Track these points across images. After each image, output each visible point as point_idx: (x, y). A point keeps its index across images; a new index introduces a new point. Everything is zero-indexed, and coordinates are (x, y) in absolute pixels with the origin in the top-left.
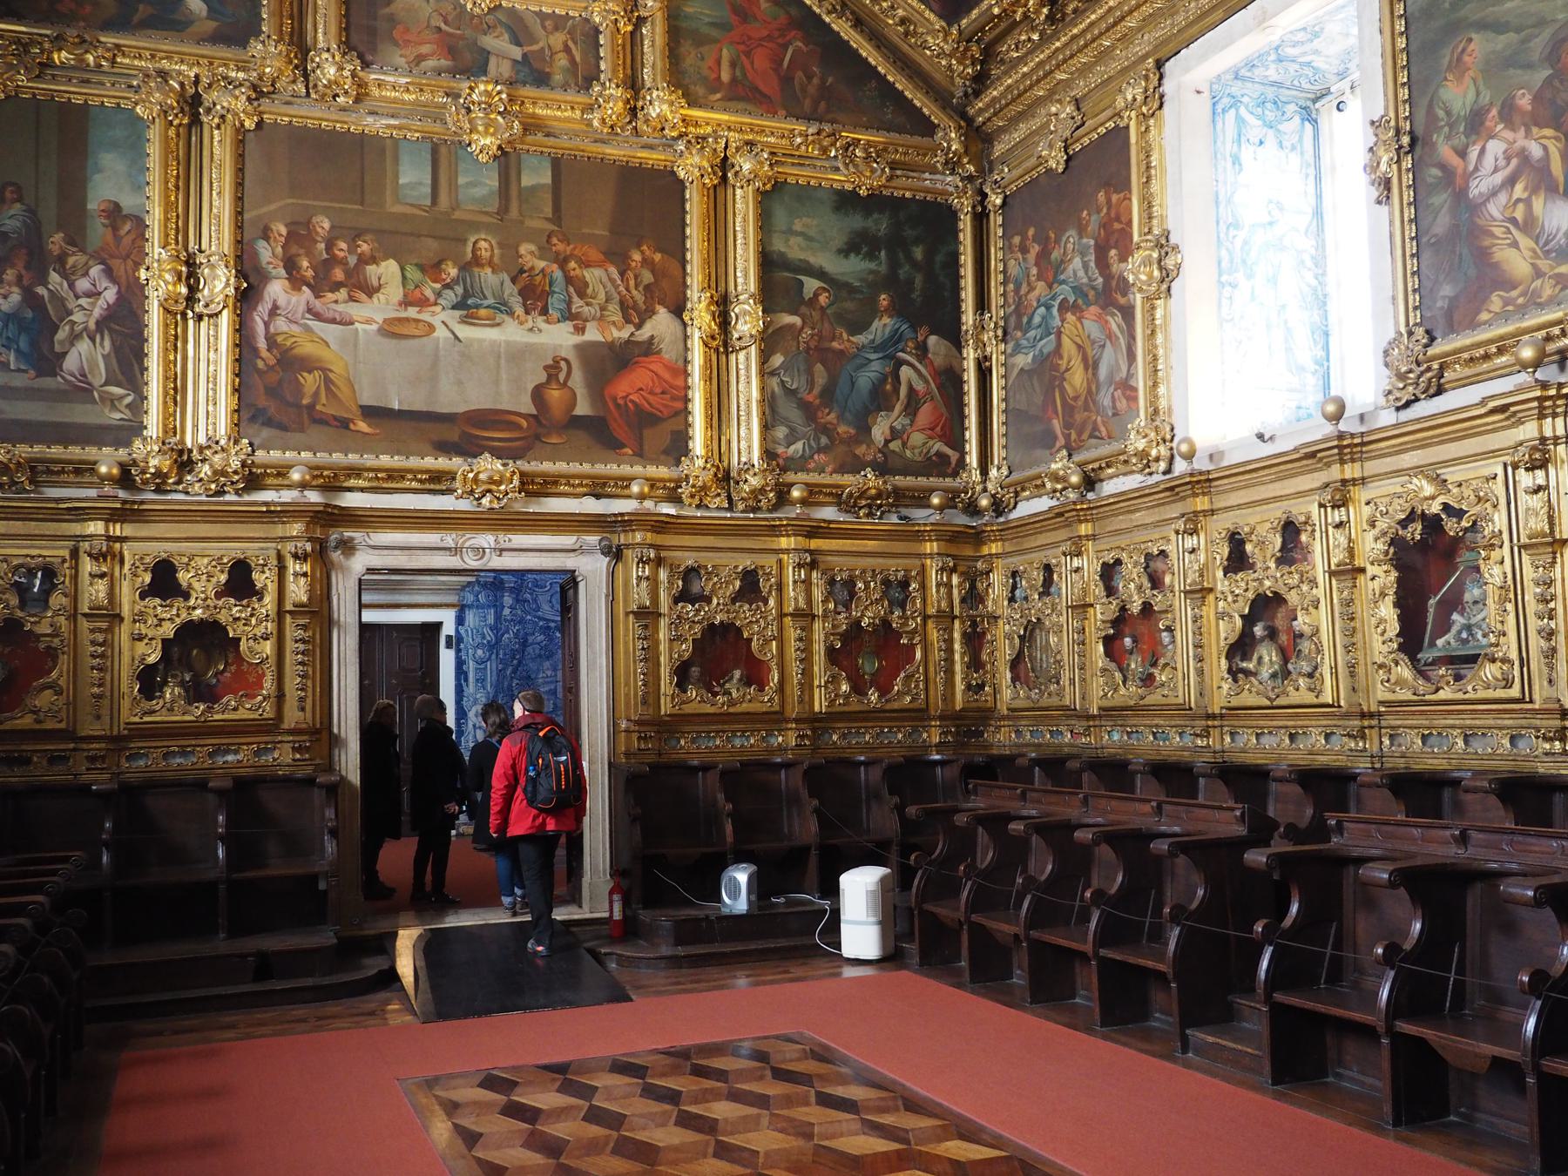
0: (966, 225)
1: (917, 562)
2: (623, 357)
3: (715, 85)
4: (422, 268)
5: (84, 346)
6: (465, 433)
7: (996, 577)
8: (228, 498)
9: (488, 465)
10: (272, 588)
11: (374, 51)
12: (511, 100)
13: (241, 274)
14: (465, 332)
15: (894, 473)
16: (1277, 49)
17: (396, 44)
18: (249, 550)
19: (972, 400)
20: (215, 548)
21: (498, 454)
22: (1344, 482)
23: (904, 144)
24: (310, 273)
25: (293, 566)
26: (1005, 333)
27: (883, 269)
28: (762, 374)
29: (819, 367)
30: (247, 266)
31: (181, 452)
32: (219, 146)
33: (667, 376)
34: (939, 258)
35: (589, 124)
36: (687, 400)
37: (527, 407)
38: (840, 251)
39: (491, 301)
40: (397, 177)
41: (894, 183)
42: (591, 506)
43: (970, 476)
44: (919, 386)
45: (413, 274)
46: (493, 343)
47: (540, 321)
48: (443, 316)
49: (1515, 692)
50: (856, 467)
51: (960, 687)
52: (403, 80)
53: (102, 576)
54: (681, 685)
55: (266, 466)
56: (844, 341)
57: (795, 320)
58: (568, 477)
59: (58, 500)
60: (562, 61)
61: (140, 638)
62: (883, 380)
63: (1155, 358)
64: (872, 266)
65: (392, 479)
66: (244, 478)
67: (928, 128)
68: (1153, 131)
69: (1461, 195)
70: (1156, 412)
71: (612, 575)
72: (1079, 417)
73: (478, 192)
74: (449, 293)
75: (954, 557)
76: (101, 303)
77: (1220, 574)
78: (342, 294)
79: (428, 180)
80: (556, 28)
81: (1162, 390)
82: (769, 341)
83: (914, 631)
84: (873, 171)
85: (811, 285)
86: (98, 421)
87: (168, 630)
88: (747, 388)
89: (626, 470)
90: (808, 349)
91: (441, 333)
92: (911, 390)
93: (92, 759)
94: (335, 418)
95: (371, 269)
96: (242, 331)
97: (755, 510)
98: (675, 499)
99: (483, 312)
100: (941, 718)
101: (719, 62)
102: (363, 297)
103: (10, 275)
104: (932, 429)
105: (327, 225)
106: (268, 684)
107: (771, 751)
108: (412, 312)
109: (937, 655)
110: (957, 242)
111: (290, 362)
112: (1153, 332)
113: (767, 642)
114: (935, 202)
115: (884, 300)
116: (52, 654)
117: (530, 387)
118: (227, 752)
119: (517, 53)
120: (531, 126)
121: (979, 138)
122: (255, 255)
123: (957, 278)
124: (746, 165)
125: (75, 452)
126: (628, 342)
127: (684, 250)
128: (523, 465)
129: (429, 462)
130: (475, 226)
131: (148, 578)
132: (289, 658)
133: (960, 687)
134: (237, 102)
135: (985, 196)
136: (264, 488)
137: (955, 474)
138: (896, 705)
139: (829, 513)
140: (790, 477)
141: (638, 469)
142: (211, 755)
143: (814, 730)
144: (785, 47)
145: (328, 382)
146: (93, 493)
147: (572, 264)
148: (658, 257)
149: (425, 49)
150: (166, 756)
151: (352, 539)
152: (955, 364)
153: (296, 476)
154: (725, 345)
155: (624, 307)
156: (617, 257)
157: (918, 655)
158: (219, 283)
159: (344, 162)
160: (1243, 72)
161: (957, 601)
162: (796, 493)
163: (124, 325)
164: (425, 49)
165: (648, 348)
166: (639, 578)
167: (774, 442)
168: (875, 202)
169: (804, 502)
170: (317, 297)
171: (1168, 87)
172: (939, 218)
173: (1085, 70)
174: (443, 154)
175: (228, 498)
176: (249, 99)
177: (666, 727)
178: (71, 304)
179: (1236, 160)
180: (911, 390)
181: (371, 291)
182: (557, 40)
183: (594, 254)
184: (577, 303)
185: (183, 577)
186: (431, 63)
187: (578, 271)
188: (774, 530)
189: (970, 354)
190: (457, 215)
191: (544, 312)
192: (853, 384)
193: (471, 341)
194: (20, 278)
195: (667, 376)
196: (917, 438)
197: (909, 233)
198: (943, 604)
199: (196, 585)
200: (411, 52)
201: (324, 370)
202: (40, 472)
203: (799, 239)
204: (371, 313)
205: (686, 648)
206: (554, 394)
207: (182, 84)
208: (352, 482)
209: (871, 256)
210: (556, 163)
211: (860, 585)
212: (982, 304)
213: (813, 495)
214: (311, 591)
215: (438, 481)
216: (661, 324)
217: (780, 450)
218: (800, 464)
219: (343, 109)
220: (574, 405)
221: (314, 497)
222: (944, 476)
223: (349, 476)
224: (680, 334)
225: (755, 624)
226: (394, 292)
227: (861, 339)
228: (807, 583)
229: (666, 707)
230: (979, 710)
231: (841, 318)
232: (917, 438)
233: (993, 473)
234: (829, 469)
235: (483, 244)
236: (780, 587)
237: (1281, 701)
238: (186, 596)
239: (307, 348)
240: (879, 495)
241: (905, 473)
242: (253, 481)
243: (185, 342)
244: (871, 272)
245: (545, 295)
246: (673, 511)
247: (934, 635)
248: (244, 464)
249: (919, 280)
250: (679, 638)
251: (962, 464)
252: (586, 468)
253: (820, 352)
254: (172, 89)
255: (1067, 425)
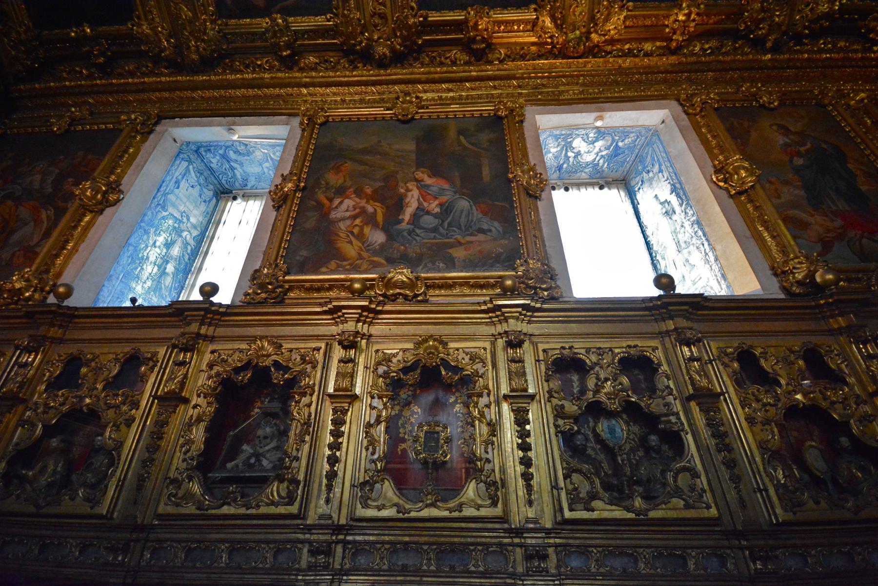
16: (227, 147)
22: (198, 335)
49: (294, 509)
171: (158, 128)
179: (177, 183)
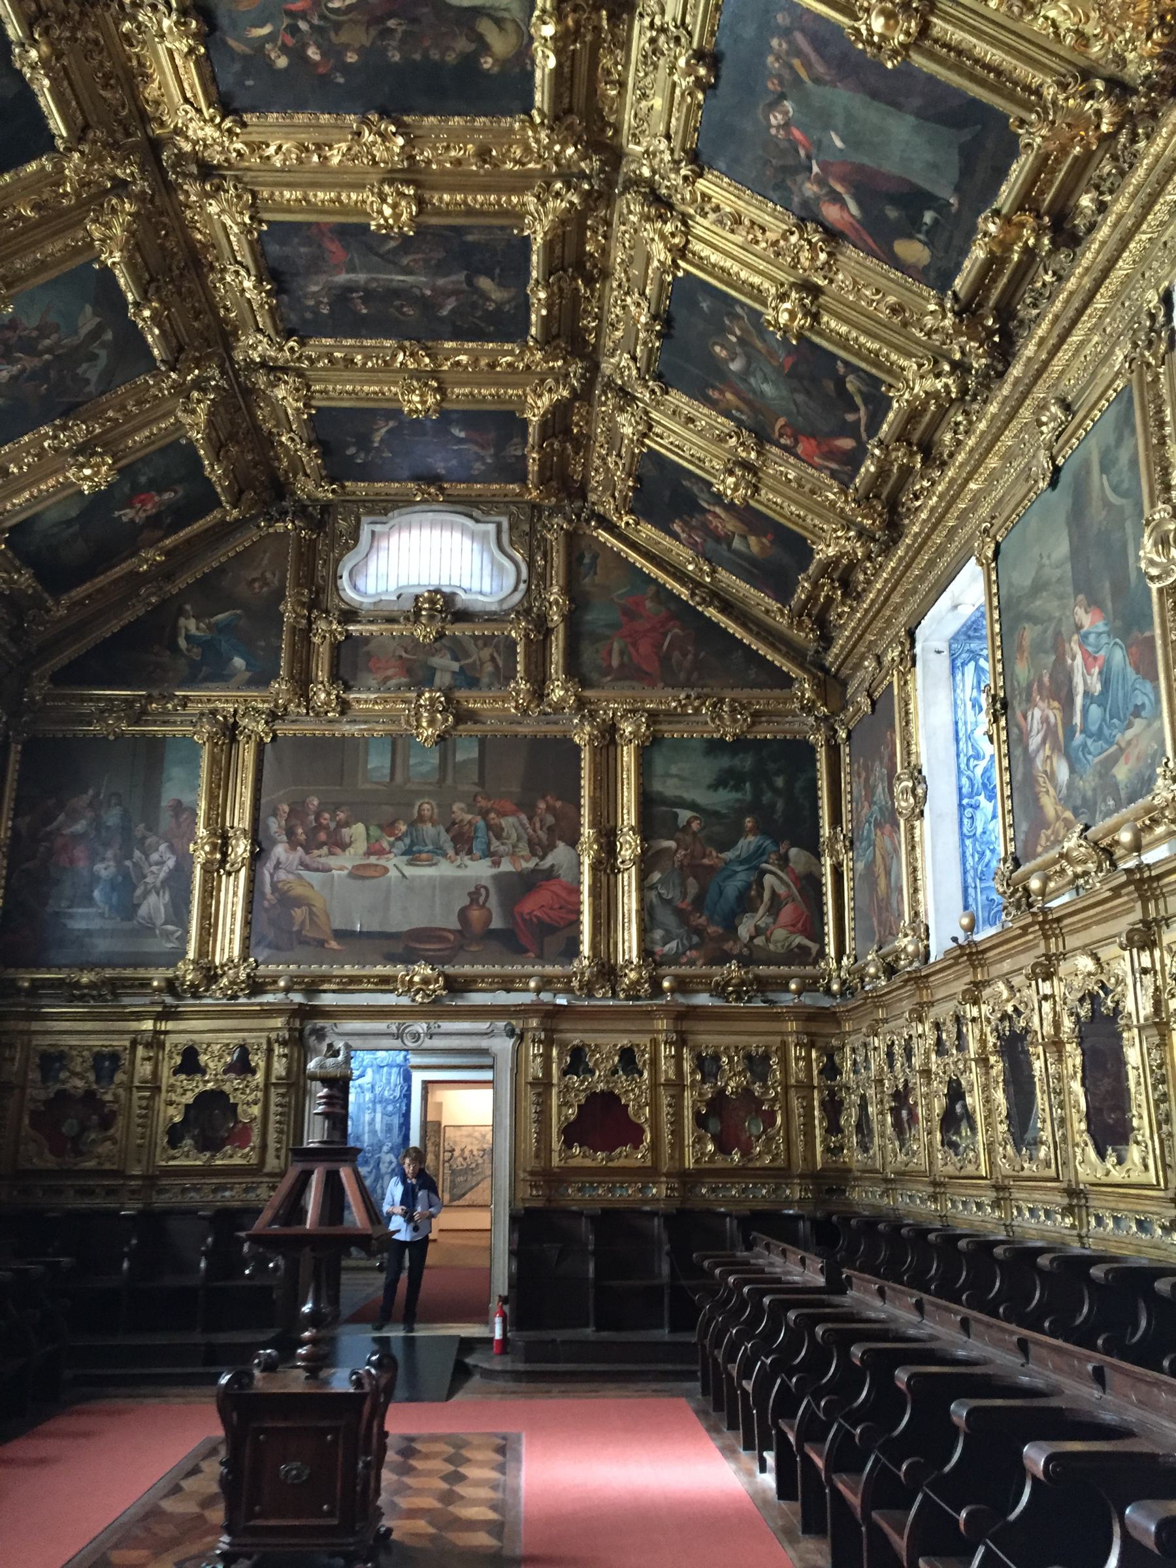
0: (822, 754)
1: (779, 1039)
2: (529, 882)
3: (608, 670)
4: (380, 827)
5: (152, 898)
6: (406, 946)
7: (848, 1050)
8: (241, 1000)
9: (423, 970)
10: (262, 1064)
11: (355, 679)
12: (449, 700)
13: (255, 842)
14: (410, 871)
15: (758, 963)
17: (370, 670)
18: (251, 1038)
19: (829, 900)
20: (226, 1038)
21: (430, 962)
23: (761, 699)
24: (303, 837)
25: (278, 1050)
26: (852, 843)
27: (749, 797)
28: (643, 886)
29: (691, 880)
30: (261, 837)
31: (209, 969)
32: (247, 754)
33: (564, 894)
34: (799, 785)
35: (508, 709)
36: (579, 913)
37: (454, 924)
38: (709, 787)
39: (430, 847)
40: (366, 763)
41: (759, 728)
42: (503, 998)
43: (827, 964)
44: (782, 891)
45: (375, 831)
46: (431, 878)
47: (466, 860)
48: (395, 861)
49: (1052, 1172)
50: (722, 959)
51: (819, 1149)
52: (373, 696)
53: (149, 1059)
54: (568, 1144)
55: (265, 977)
56: (713, 858)
57: (672, 844)
58: (483, 978)
59: (125, 1007)
60: (489, 668)
61: (171, 1103)
62: (749, 886)
63: (915, 870)
64: (739, 795)
65: (350, 984)
66: (248, 986)
67: (786, 681)
68: (910, 685)
69: (1026, 748)
70: (917, 914)
71: (516, 1052)
72: (884, 915)
73: (425, 769)
74: (400, 844)
75: (808, 1034)
76: (165, 869)
77: (933, 1057)
78: (325, 849)
79: (388, 764)
80: (485, 645)
81: (920, 896)
82: (646, 863)
83: (775, 1099)
84: (735, 721)
85: (684, 815)
86: (155, 949)
87: (189, 1098)
88: (629, 902)
89: (529, 969)
90: (682, 867)
91: (393, 873)
92: (774, 893)
93: (133, 1192)
94: (315, 939)
95: (345, 831)
96: (252, 881)
97: (638, 998)
98: (569, 990)
99: (424, 856)
100: (801, 1176)
101: (610, 653)
102: (338, 850)
103: (109, 854)
104: (794, 925)
105: (316, 802)
106: (255, 1140)
107: (645, 1201)
108: (373, 860)
109: (798, 1121)
110: (816, 770)
111: (287, 901)
112: (913, 848)
113: (641, 1107)
114: (794, 740)
115: (748, 822)
116: (113, 1114)
117: (457, 909)
118: (226, 1189)
119: (455, 666)
120: (463, 716)
121: (832, 685)
122: (267, 827)
123: (816, 799)
124: (627, 728)
125: (142, 973)
126: (534, 871)
127: (579, 797)
128: (448, 969)
129: (380, 970)
130: (419, 794)
131: (178, 1060)
132: (273, 1118)
133: (819, 1149)
134: (261, 727)
135: (836, 731)
136: (266, 992)
137: (815, 963)
138: (758, 1164)
139: (703, 999)
140: (665, 970)
141: (538, 968)
142: (215, 1191)
143: (683, 1184)
144: (665, 635)
145: (311, 913)
146: (147, 1000)
147: (492, 815)
148: (558, 804)
149: (390, 672)
150: (184, 1191)
151: (323, 1028)
152: (814, 869)
153: (282, 984)
154: (614, 866)
155: (531, 843)
156: (527, 807)
157: (779, 1120)
158: (241, 848)
159: (331, 757)
160: (971, 633)
161: (815, 1073)
162: (666, 984)
163: (179, 880)
164: (390, 672)
165: (550, 874)
166: (535, 1056)
167: (653, 942)
168: (740, 745)
169: (672, 990)
170: (307, 853)
171: (918, 650)
172: (798, 754)
173: (881, 632)
174: (399, 744)
175: (241, 1000)
176: (267, 723)
177: (550, 1179)
178: (146, 871)
180: (774, 893)
181: (344, 846)
182: (486, 653)
183: (509, 806)
184: (495, 844)
185: (203, 1059)
186: (393, 682)
187: (496, 821)
188: (649, 1015)
189: (828, 862)
190: (408, 786)
191: (470, 852)
192: (721, 893)
193: (414, 878)
194: (115, 856)
195: (564, 894)
196: (779, 934)
197: (772, 766)
198: (802, 1075)
199: (211, 1065)
200: (380, 676)
201: (310, 905)
202: (116, 987)
203: (675, 780)
204: (343, 863)
205: (572, 1113)
206: (475, 914)
207: (225, 717)
208: (326, 986)
209: (737, 788)
210: (483, 742)
211: (725, 1059)
212: (836, 820)
213: (683, 985)
214: (289, 1070)
215: (385, 983)
216: (560, 854)
217: (657, 949)
218: (674, 960)
219: (330, 721)
220: (489, 920)
221: (297, 998)
222: (805, 965)
223: (323, 982)
224: (575, 862)
225: (633, 1094)
226: (361, 846)
227: (729, 855)
228: (678, 1058)
229: (556, 1161)
230: (837, 1170)
231: (711, 840)
232: (779, 934)
233: (845, 961)
234: (700, 962)
235: (426, 806)
236: (654, 1062)
237: (963, 1173)
238: (204, 1073)
239: (298, 890)
240: (743, 983)
241: (768, 963)
242: (256, 986)
243: (219, 890)
244: (738, 800)
245: (471, 840)
246: (564, 1002)
247: (796, 1103)
248: (248, 975)
249: (780, 805)
250: (567, 1104)
251: (822, 954)
252: (497, 969)
253: (693, 868)
254: (217, 721)
255: (880, 923)
